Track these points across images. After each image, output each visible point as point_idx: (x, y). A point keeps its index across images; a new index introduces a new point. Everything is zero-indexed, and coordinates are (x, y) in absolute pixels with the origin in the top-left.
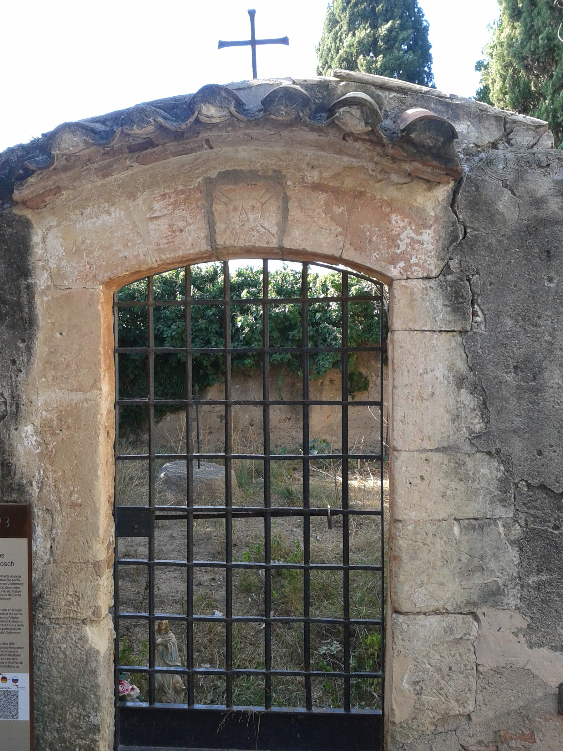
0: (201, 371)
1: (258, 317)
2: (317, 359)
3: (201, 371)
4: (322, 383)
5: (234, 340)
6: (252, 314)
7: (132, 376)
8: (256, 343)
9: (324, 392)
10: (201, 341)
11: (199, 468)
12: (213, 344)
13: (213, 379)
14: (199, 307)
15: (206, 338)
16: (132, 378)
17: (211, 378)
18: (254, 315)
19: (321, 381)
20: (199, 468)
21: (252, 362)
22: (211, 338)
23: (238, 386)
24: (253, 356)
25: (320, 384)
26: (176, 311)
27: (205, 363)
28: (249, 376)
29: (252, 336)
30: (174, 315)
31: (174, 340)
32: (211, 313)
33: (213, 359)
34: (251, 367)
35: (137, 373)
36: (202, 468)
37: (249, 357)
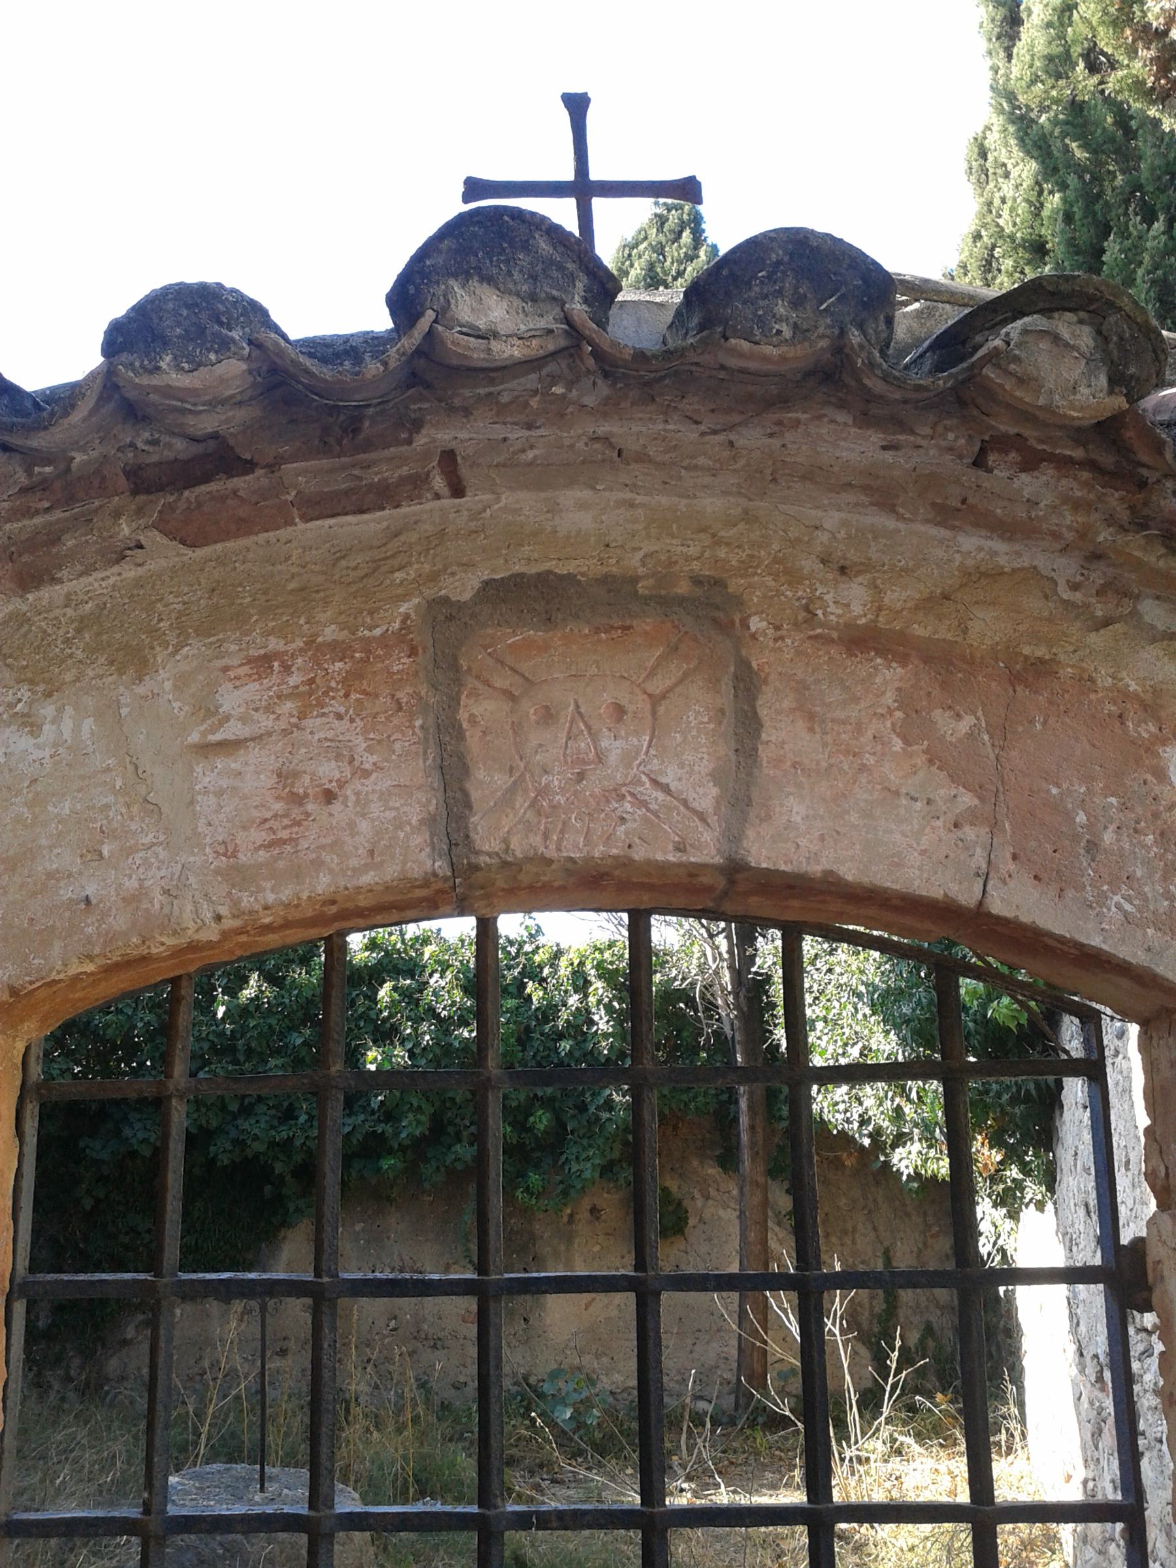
0: (268, 1188)
1: (417, 1051)
2: (563, 1158)
3: (268, 1188)
4: (571, 1216)
5: (356, 1108)
6: (402, 1043)
7: (88, 1204)
8: (411, 1116)
9: (577, 1241)
10: (273, 1112)
11: (262, 1489)
12: (303, 1118)
13: (298, 1210)
14: (270, 1026)
15: (286, 1104)
16: (88, 1208)
17: (291, 1207)
18: (409, 1045)
19: (569, 1211)
20: (262, 1489)
21: (398, 1164)
22: (297, 1105)
23: (359, 1227)
24: (403, 1149)
25: (565, 1219)
26: (211, 1037)
27: (279, 1168)
28: (389, 1200)
29: (402, 1099)
30: (206, 1046)
31: (203, 1110)
32: (299, 1041)
33: (298, 1158)
34: (395, 1178)
35: (101, 1196)
36: (272, 1487)
37: (390, 1152)
